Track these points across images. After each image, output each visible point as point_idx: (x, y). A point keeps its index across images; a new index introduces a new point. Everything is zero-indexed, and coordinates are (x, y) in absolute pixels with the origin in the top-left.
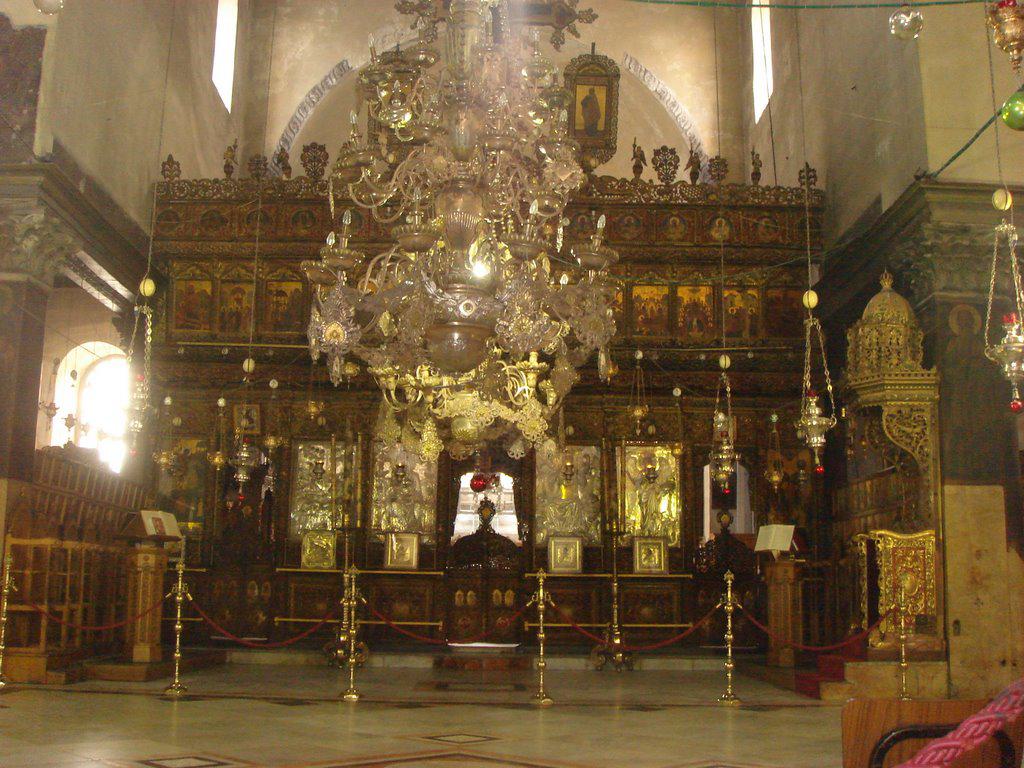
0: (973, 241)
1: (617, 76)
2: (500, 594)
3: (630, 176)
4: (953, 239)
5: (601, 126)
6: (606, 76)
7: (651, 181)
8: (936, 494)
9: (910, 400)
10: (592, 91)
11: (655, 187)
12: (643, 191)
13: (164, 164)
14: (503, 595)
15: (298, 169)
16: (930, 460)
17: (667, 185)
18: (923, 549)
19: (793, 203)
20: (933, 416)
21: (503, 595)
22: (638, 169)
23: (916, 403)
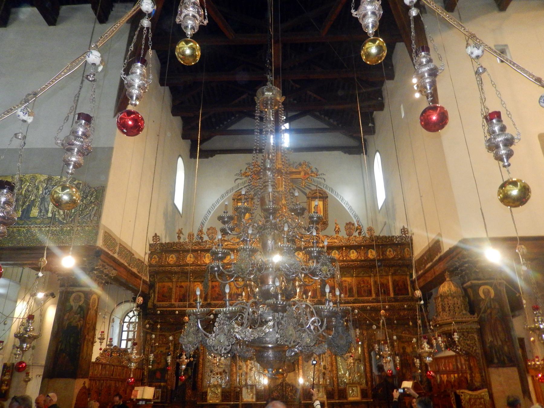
8: (485, 372)
13: (153, 237)
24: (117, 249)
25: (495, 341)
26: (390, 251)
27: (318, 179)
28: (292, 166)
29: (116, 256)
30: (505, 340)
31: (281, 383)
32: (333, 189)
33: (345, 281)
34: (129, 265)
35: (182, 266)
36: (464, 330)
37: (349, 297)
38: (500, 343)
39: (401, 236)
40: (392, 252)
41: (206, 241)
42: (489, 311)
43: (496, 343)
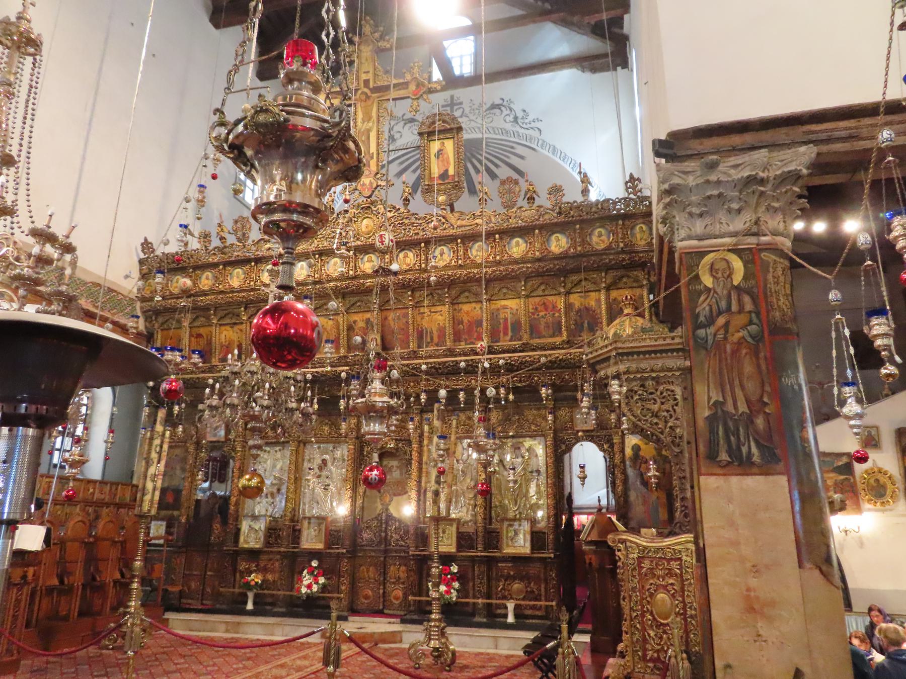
8: (692, 487)
9: (652, 371)
15: (231, 239)
18: (680, 559)
20: (685, 388)
23: (662, 374)
25: (730, 401)
26: (600, 235)
27: (526, 132)
30: (760, 399)
32: (558, 146)
33: (505, 307)
35: (193, 295)
36: (646, 375)
37: (511, 341)
38: (743, 408)
39: (625, 199)
40: (604, 238)
41: (232, 245)
42: (721, 321)
43: (730, 407)
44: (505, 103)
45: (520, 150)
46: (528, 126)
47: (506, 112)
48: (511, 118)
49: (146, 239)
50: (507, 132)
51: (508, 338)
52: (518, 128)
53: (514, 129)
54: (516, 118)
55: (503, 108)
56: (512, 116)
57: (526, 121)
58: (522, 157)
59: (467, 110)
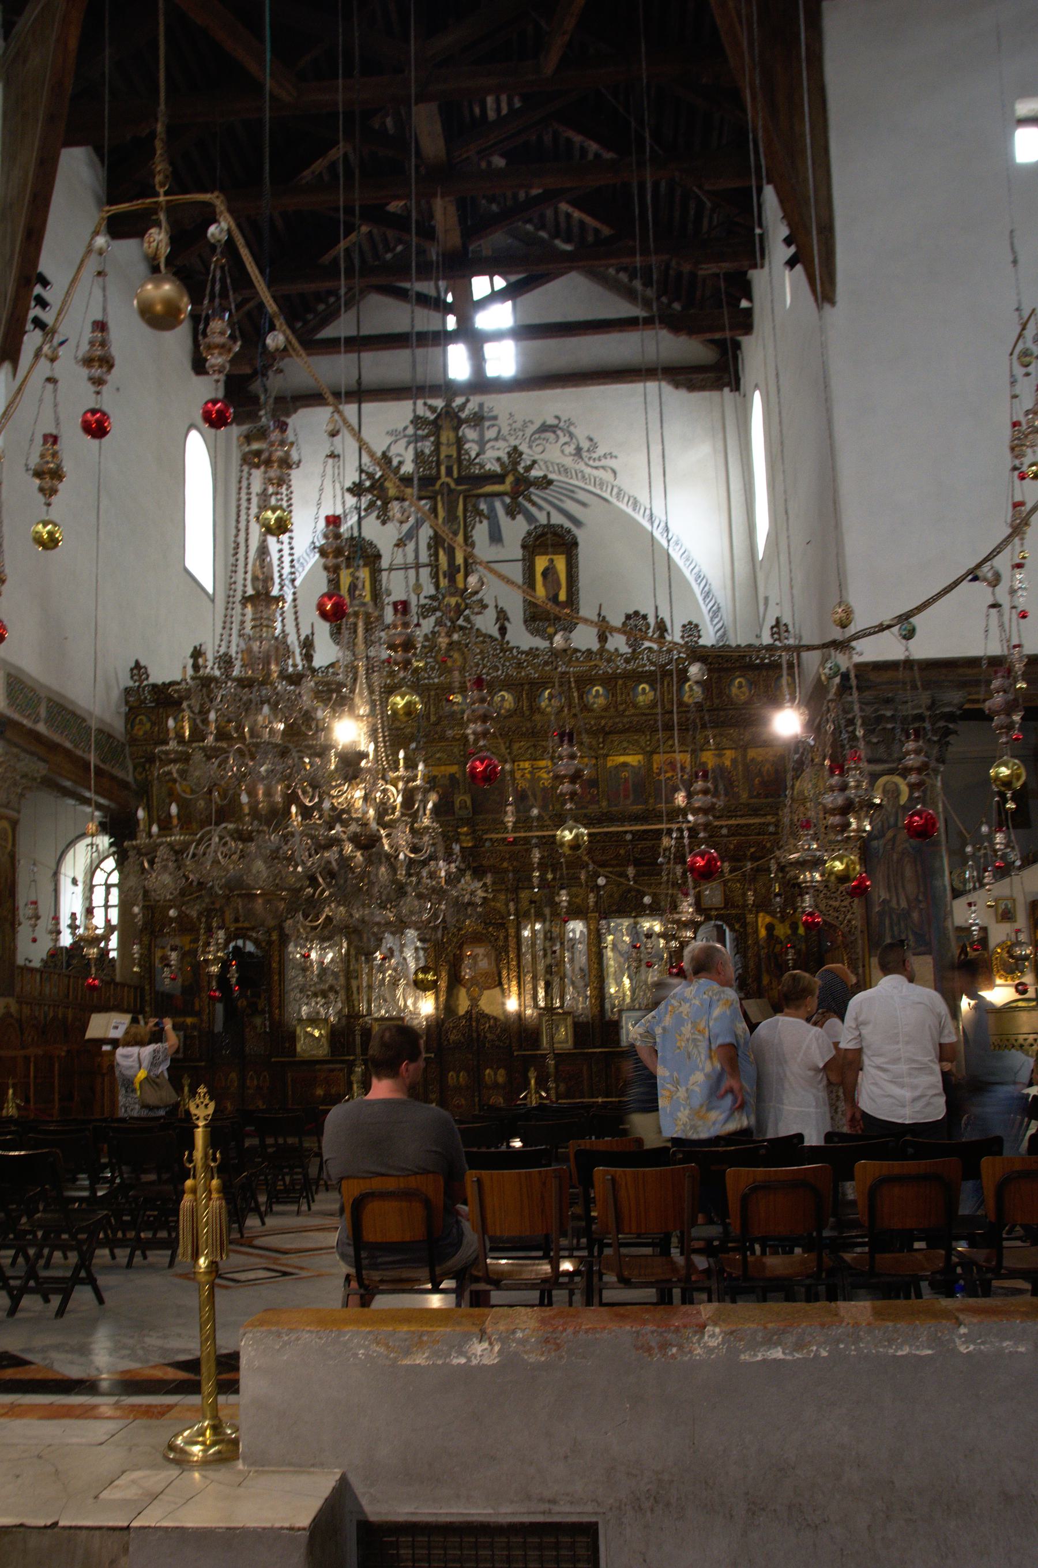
0: (896, 710)
1: (575, 544)
2: (492, 1073)
3: (595, 646)
4: (876, 711)
5: (562, 596)
6: (563, 544)
7: (616, 650)
8: (864, 966)
10: (551, 561)
11: (622, 655)
12: (609, 661)
14: (495, 1074)
16: (858, 933)
17: (634, 651)
19: (767, 661)
21: (495, 1074)
22: (603, 638)
24: (43, 712)
26: (740, 686)
27: (595, 472)
28: (521, 433)
29: (41, 728)
30: (917, 899)
31: (467, 1012)
33: (625, 765)
34: (76, 746)
38: (904, 904)
42: (890, 834)
43: (894, 904)
44: (562, 424)
45: (581, 496)
46: (597, 464)
47: (564, 439)
48: (570, 449)
49: (137, 663)
50: (566, 470)
51: (629, 802)
52: (581, 466)
53: (577, 467)
54: (579, 450)
55: (559, 432)
56: (573, 447)
57: (595, 456)
58: (584, 505)
59: (505, 431)
